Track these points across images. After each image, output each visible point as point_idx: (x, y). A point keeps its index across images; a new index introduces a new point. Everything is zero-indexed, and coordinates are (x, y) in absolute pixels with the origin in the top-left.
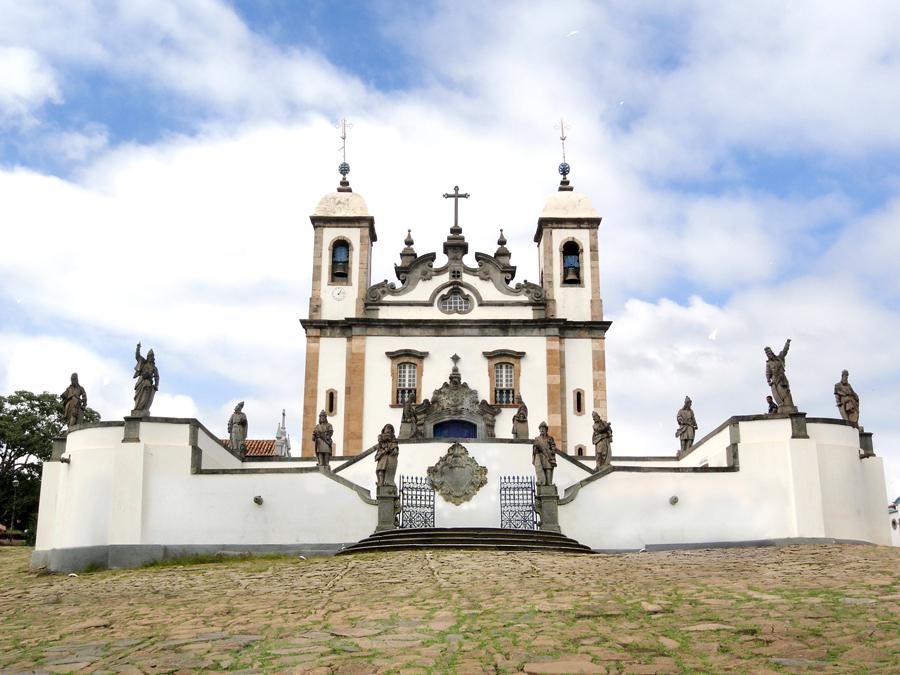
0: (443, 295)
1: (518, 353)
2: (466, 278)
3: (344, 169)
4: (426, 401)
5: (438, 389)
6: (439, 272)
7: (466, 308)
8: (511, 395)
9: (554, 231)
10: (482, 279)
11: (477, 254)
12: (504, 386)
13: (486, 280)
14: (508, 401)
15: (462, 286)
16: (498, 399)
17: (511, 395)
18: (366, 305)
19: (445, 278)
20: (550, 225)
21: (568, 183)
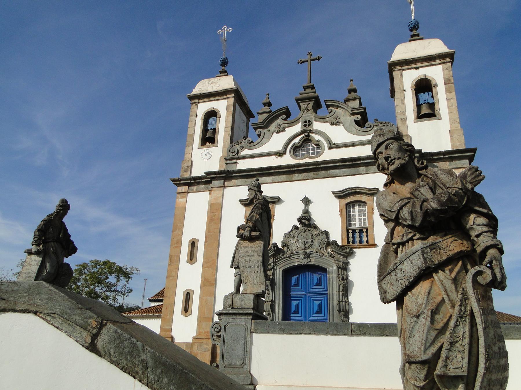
0: (295, 143)
1: (370, 190)
2: (317, 125)
3: (224, 63)
4: (275, 245)
5: (287, 233)
6: (291, 124)
7: (317, 153)
8: (364, 234)
9: (404, 72)
10: (332, 124)
11: (326, 101)
12: (357, 225)
13: (336, 125)
14: (361, 242)
15: (313, 133)
16: (351, 239)
17: (364, 234)
18: (226, 160)
19: (297, 128)
20: (400, 68)
21: (418, 35)
